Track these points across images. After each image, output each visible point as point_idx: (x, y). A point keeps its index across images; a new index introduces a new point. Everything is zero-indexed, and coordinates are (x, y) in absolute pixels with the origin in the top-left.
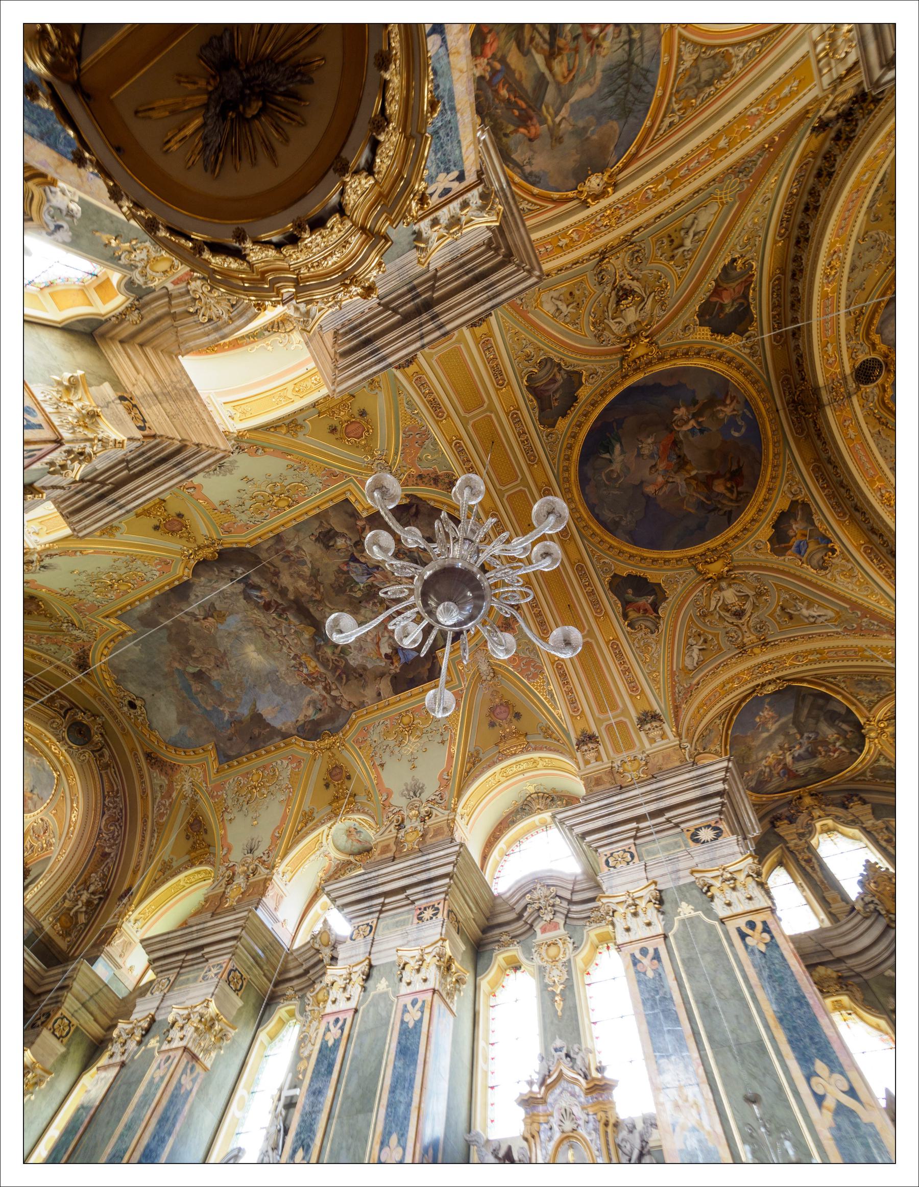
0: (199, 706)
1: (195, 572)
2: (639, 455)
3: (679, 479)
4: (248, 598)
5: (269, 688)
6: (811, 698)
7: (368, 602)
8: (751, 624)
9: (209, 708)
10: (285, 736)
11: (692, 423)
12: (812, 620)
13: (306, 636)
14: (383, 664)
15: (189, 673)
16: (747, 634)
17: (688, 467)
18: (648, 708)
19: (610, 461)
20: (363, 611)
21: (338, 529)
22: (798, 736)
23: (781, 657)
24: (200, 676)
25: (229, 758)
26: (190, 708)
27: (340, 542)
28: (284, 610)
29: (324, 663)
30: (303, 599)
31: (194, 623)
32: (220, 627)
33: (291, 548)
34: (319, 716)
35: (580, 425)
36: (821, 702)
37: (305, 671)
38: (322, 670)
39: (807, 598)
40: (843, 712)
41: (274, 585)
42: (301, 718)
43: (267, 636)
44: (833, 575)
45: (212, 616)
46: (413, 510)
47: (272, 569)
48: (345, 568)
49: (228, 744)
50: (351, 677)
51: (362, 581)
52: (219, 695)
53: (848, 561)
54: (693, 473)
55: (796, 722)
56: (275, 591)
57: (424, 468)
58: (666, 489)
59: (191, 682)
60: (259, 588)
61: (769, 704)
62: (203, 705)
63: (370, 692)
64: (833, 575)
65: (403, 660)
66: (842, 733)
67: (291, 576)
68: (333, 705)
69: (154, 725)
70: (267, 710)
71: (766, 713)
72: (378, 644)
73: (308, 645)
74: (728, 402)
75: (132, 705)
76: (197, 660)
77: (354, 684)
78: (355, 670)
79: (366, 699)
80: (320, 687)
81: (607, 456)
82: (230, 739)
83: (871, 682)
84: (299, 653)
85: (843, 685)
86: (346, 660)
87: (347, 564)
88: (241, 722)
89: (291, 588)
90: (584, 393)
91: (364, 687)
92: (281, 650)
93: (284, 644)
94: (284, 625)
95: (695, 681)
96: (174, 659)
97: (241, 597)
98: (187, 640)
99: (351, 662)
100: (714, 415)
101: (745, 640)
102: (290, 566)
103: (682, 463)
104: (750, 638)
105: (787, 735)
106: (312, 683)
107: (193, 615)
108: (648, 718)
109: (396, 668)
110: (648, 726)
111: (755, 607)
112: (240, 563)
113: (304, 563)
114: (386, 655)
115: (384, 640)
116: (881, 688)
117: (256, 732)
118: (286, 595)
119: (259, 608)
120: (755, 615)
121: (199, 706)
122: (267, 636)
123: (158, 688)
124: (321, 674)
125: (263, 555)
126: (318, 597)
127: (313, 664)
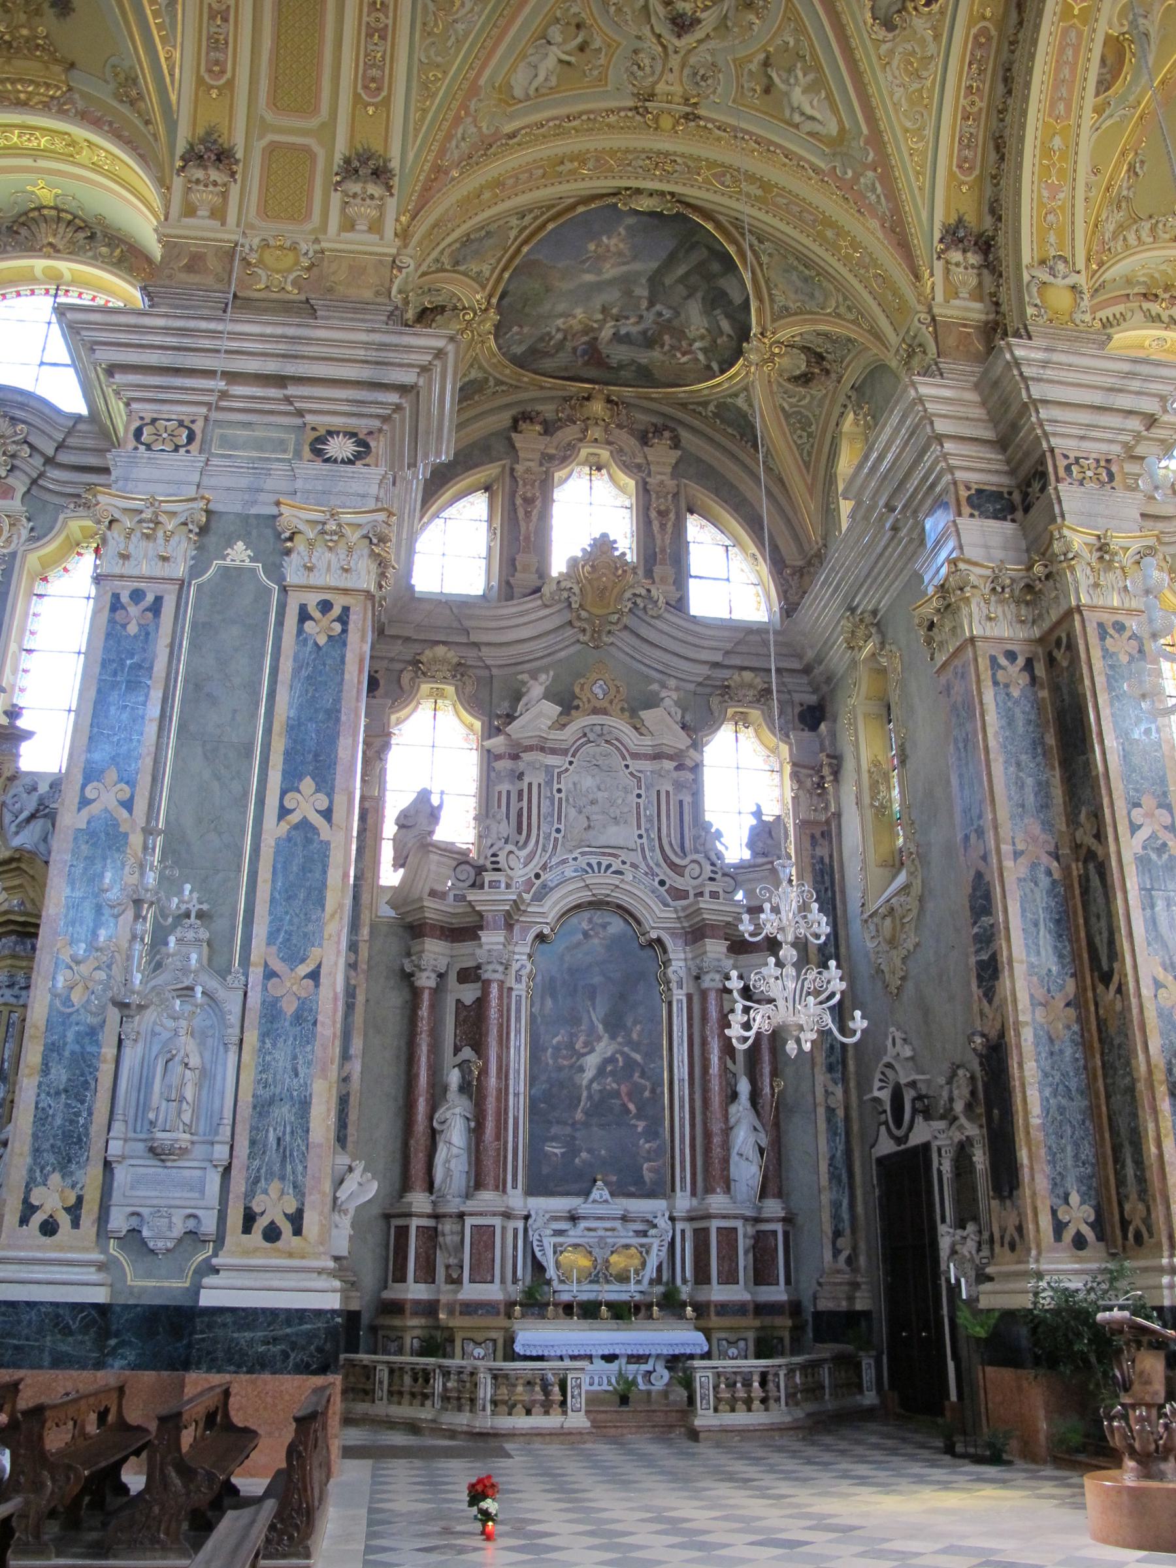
6: (705, 253)
8: (692, 60)
12: (797, 118)
16: (670, 77)
18: (377, 146)
22: (644, 304)
23: (699, 159)
36: (716, 267)
39: (819, 68)
40: (737, 299)
44: (892, 52)
53: (937, 37)
55: (655, 281)
61: (629, 228)
64: (892, 52)
66: (715, 331)
71: (613, 242)
83: (806, 280)
85: (765, 259)
95: (508, 128)
101: (661, 88)
104: (671, 86)
105: (628, 293)
108: (367, 167)
110: (355, 187)
111: (723, 25)
116: (812, 296)
120: (712, 44)
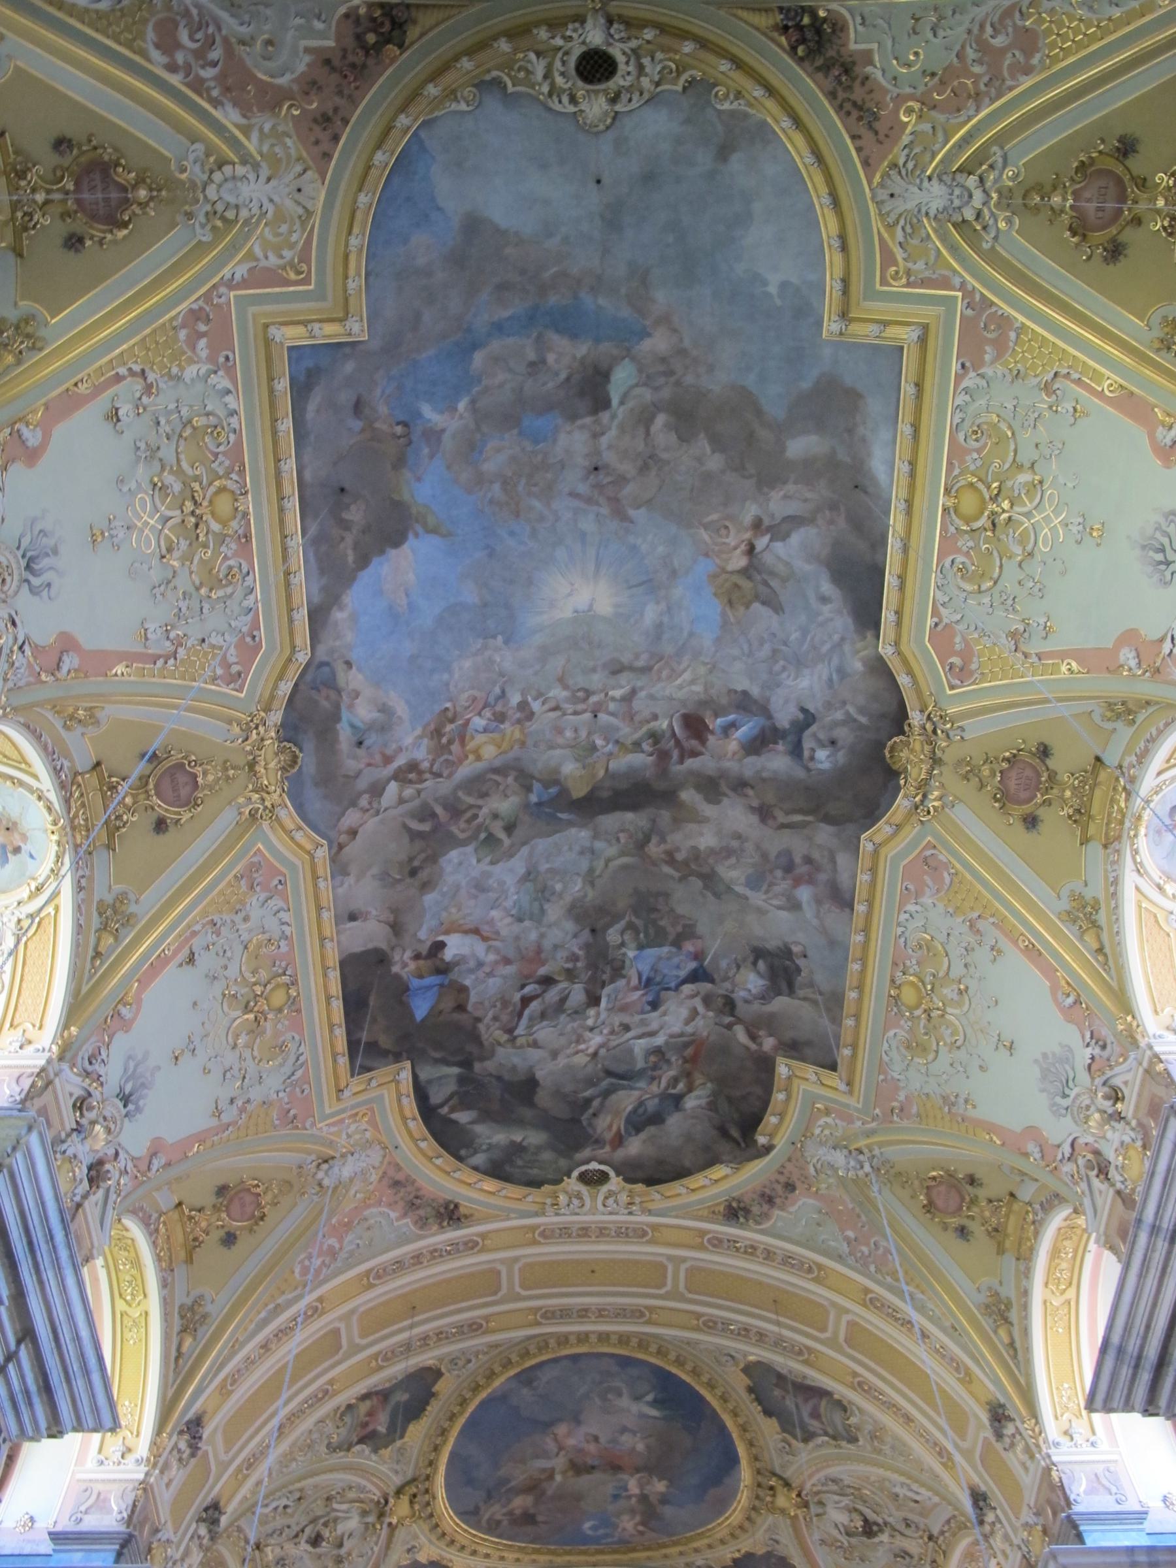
0: (499, 328)
1: (880, 669)
2: (624, 1430)
3: (559, 1463)
4: (744, 703)
5: (470, 594)
7: (587, 946)
9: (478, 358)
10: (318, 617)
11: (636, 1491)
13: (569, 768)
14: (422, 934)
15: (615, 360)
17: (570, 1473)
19: (637, 1398)
20: (570, 926)
21: (781, 1003)
24: (591, 390)
25: (301, 390)
26: (503, 287)
27: (752, 982)
28: (663, 756)
29: (479, 785)
30: (665, 816)
31: (751, 511)
32: (704, 567)
33: (804, 894)
34: (344, 734)
35: (724, 1399)
37: (479, 722)
38: (465, 770)
41: (741, 785)
42: (353, 679)
43: (617, 669)
45: (745, 572)
46: (735, 1133)
47: (782, 818)
48: (689, 947)
49: (346, 397)
50: (419, 844)
51: (640, 961)
52: (509, 419)
54: (558, 1478)
56: (723, 774)
57: (803, 1205)
58: (551, 1446)
59: (583, 349)
60: (757, 745)
62: (496, 345)
63: (365, 891)
65: (415, 983)
67: (738, 836)
68: (362, 784)
69: (492, 104)
70: (403, 568)
72: (476, 931)
73: (542, 760)
74: (641, 1528)
75: (595, 67)
76: (644, 419)
77: (399, 849)
78: (433, 859)
79: (351, 880)
80: (422, 754)
81: (650, 1397)
82: (358, 407)
84: (533, 726)
86: (464, 843)
87: (698, 956)
88: (400, 462)
89: (708, 810)
90: (769, 1428)
91: (384, 876)
92: (562, 681)
93: (574, 700)
94: (626, 732)
96: (682, 352)
97: (755, 691)
98: (718, 444)
99: (454, 855)
100: (632, 1512)
102: (765, 856)
103: (578, 1468)
106: (438, 733)
107: (779, 530)
109: (403, 964)
112: (841, 777)
113: (754, 883)
114: (441, 945)
115: (480, 948)
117: (355, 514)
118: (698, 788)
119: (705, 703)
121: (499, 328)
122: (617, 669)
123: (612, 219)
124: (453, 765)
125: (825, 834)
126: (654, 849)
127: (489, 752)
